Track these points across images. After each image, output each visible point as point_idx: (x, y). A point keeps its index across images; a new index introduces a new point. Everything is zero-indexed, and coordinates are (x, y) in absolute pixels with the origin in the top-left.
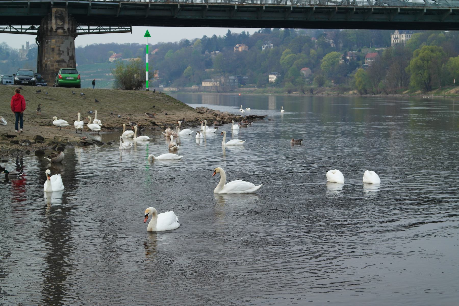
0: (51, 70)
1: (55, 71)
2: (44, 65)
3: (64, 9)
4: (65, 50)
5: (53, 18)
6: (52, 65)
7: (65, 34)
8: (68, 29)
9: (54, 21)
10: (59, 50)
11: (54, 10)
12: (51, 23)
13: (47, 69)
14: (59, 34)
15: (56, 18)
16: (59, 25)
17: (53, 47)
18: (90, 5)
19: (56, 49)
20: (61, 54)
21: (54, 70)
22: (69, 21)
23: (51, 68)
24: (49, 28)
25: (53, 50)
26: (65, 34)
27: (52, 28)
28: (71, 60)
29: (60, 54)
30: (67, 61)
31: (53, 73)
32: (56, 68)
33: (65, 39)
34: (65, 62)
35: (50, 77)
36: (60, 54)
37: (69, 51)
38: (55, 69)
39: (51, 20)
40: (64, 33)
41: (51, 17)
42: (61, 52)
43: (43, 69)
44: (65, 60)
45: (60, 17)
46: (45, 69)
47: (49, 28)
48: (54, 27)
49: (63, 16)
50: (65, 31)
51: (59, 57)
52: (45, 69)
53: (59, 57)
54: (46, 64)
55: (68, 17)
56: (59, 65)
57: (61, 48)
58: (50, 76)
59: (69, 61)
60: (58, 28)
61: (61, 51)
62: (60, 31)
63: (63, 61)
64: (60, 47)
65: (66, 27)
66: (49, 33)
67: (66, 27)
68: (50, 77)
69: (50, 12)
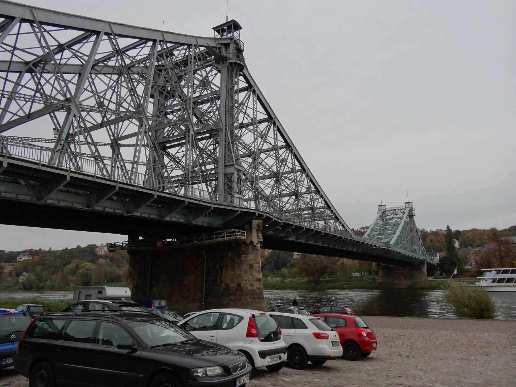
0: (250, 290)
1: (257, 291)
6: (252, 285)
9: (254, 234)
11: (255, 222)
16: (260, 239)
21: (254, 291)
32: (257, 288)
38: (255, 289)
41: (251, 229)
58: (250, 298)
66: (243, 248)
69: (250, 223)
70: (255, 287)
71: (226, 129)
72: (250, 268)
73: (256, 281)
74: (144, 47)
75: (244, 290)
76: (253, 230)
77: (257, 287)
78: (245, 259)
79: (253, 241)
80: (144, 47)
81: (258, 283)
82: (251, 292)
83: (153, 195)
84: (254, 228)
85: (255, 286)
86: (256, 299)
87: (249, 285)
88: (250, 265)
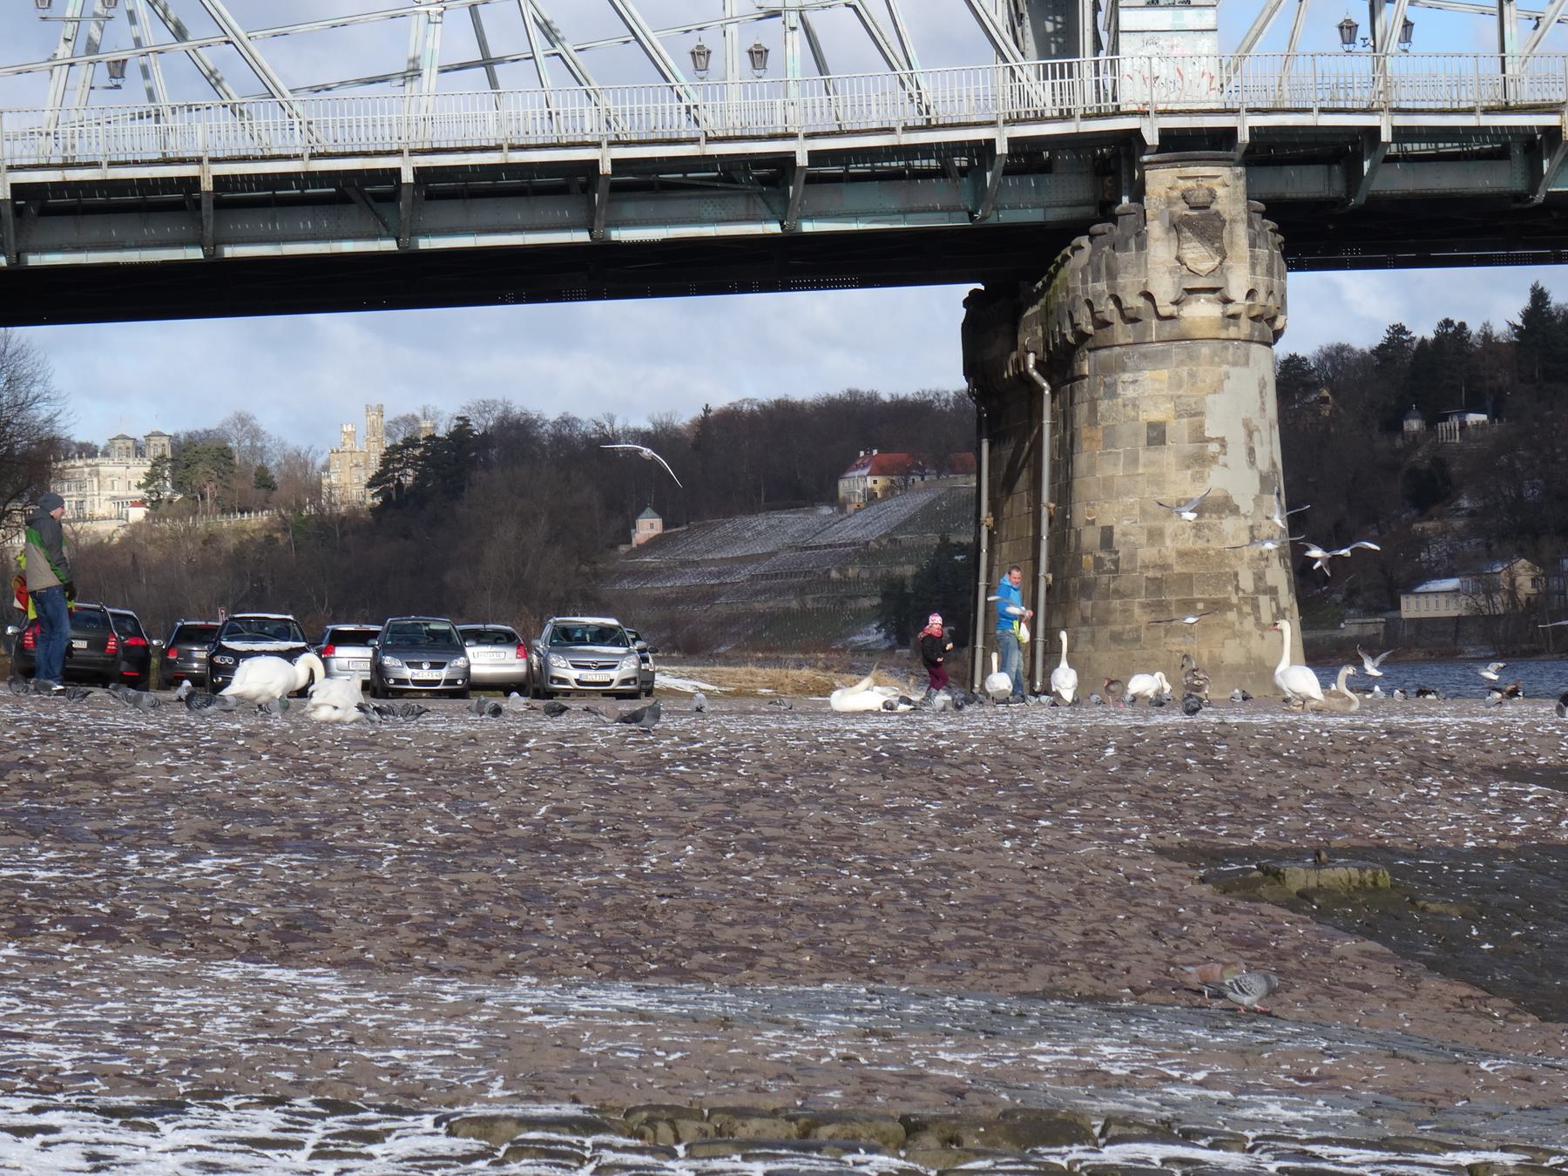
0: (1146, 567)
1: (1178, 569)
2: (1090, 538)
3: (1225, 172)
4: (1237, 438)
5: (1155, 229)
6: (1155, 535)
7: (1232, 332)
9: (1160, 249)
10: (1200, 438)
12: (1142, 265)
13: (1116, 562)
15: (1177, 226)
16: (1196, 274)
17: (1156, 416)
18: (1386, 136)
19: (1179, 430)
20: (1214, 459)
21: (1164, 567)
22: (1253, 245)
23: (1147, 554)
25: (1157, 435)
26: (1232, 332)
28: (1266, 497)
30: (1246, 505)
31: (1157, 585)
32: (1182, 554)
33: (1235, 364)
35: (1137, 611)
36: (1199, 461)
37: (1256, 434)
38: (1172, 558)
39: (1142, 246)
40: (1226, 327)
42: (1213, 448)
43: (1088, 560)
44: (1237, 500)
46: (1099, 562)
48: (1164, 291)
49: (1217, 214)
51: (1198, 478)
52: (1099, 562)
53: (1198, 478)
54: (1107, 536)
55: (1250, 224)
57: (1208, 423)
58: (1144, 606)
59: (1258, 501)
61: (1212, 440)
62: (1202, 311)
63: (1226, 506)
64: (1201, 414)
65: (1238, 284)
67: (1238, 284)
68: (1137, 611)
70: (1170, 547)
75: (1123, 565)
77: (1180, 546)
82: (1150, 574)
84: (1156, 217)
85: (1168, 542)
86: (1173, 608)
87: (1143, 539)
88: (1152, 426)
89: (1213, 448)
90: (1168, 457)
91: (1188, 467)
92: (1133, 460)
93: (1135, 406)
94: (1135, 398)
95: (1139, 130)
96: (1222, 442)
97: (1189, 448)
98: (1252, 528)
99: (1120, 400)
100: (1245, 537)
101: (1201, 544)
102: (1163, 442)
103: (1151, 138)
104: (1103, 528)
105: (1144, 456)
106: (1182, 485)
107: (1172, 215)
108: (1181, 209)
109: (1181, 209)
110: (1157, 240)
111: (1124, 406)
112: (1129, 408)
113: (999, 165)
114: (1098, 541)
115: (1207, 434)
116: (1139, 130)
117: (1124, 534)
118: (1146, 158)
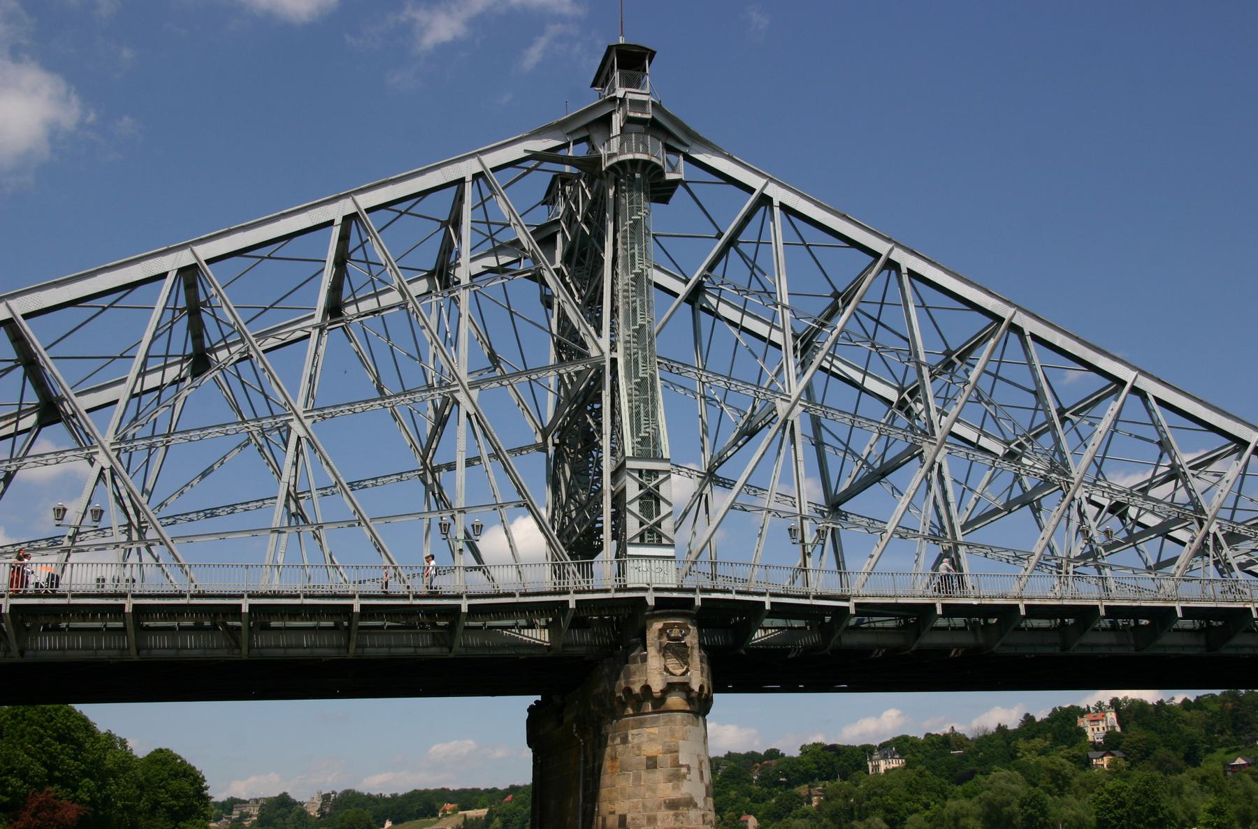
5: (652, 652)
8: (701, 688)
9: (654, 661)
14: (675, 708)
15: (664, 651)
18: (768, 607)
20: (684, 776)
24: (637, 689)
25: (652, 763)
27: (647, 688)
29: (676, 776)
30: (701, 804)
34: (695, 806)
36: (676, 776)
39: (644, 659)
42: (684, 770)
44: (696, 800)
45: (676, 650)
47: (637, 689)
48: (657, 685)
50: (693, 695)
51: (676, 788)
53: (676, 788)
56: (676, 815)
60: (670, 688)
61: (682, 766)
71: (614, 362)
72: (648, 767)
73: (663, 808)
74: (535, 168)
76: (649, 649)
78: (636, 741)
79: (648, 683)
80: (535, 168)
81: (672, 812)
83: (763, 603)
84: (652, 645)
85: (659, 824)
87: (645, 822)
88: (649, 758)
89: (684, 770)
90: (659, 775)
91: (670, 781)
92: (638, 778)
93: (639, 748)
94: (640, 744)
95: (644, 598)
96: (689, 768)
97: (670, 770)
98: (703, 815)
99: (630, 745)
100: (700, 820)
101: (678, 825)
102: (656, 767)
103: (651, 602)
104: (620, 816)
105: (644, 774)
106: (667, 791)
107: (660, 643)
108: (665, 640)
109: (665, 640)
110: (652, 657)
111: (633, 747)
112: (635, 749)
113: (569, 616)
114: (617, 824)
115: (680, 762)
116: (644, 598)
117: (633, 819)
118: (647, 613)
